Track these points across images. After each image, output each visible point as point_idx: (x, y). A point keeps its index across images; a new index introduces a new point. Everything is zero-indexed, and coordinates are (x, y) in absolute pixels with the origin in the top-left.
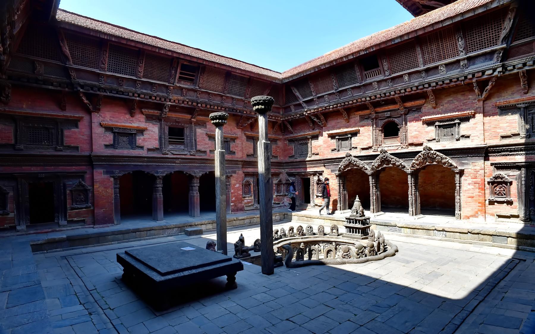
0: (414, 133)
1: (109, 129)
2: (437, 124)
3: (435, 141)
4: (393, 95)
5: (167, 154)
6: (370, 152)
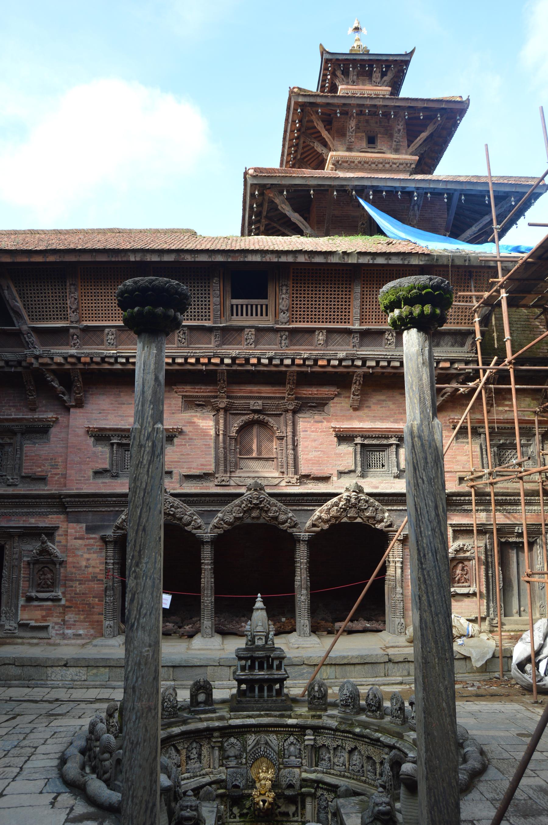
0: (312, 455)
2: (358, 440)
3: (352, 474)
4: (287, 366)
6: (211, 488)
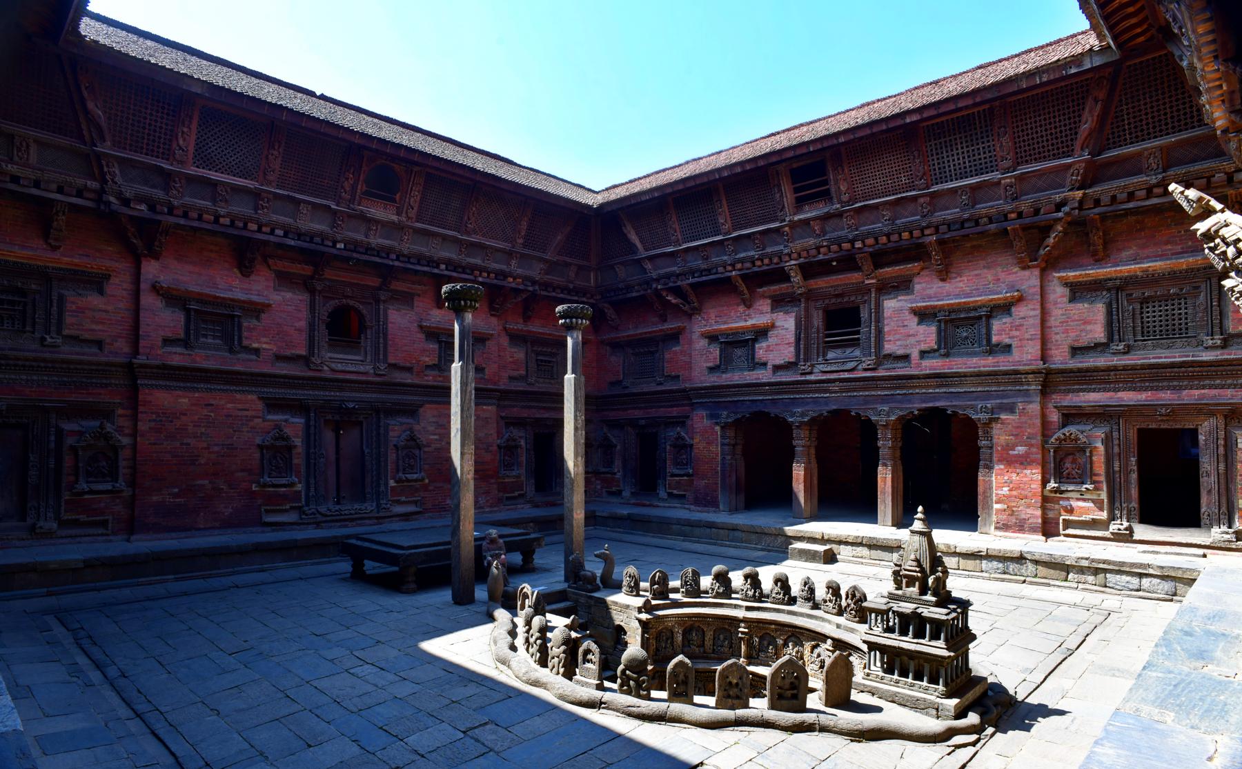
1: (712, 338)
5: (811, 373)
